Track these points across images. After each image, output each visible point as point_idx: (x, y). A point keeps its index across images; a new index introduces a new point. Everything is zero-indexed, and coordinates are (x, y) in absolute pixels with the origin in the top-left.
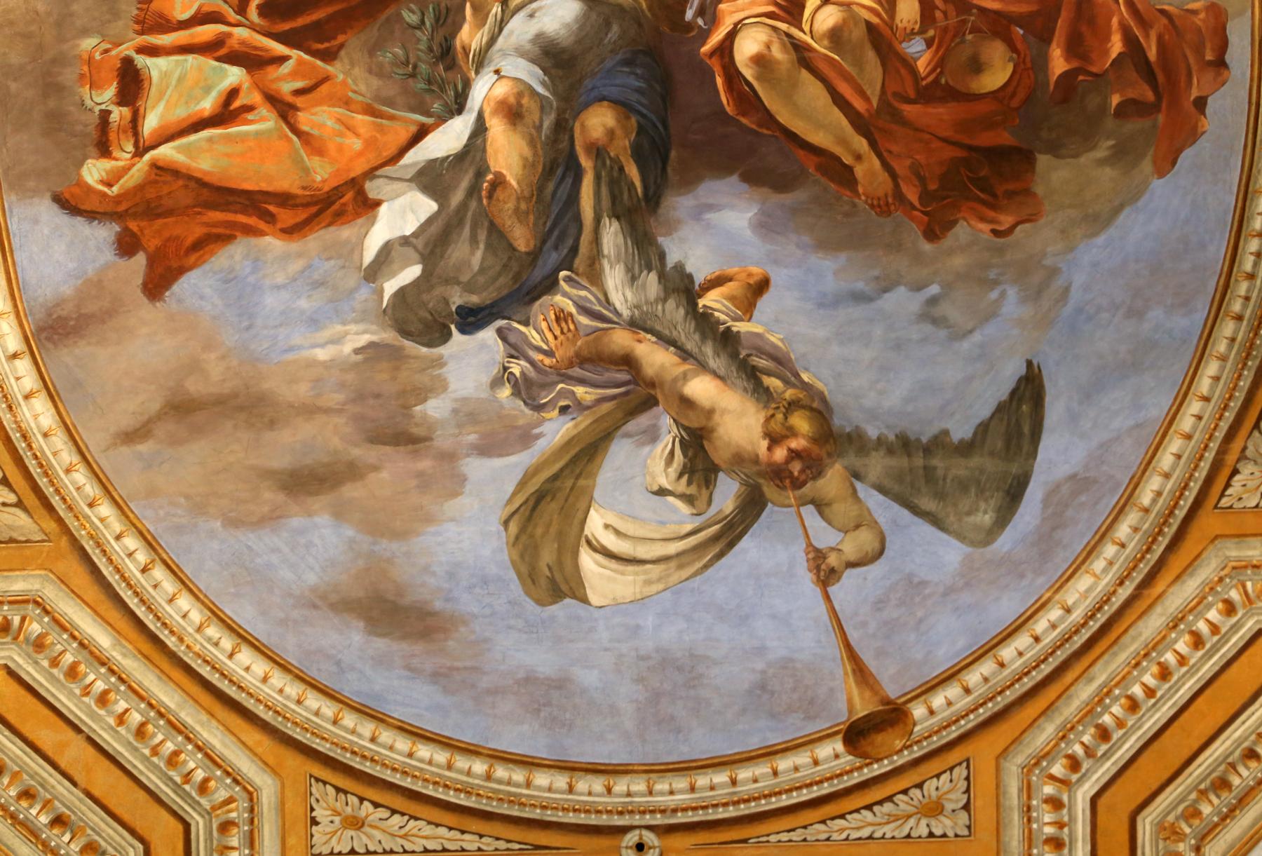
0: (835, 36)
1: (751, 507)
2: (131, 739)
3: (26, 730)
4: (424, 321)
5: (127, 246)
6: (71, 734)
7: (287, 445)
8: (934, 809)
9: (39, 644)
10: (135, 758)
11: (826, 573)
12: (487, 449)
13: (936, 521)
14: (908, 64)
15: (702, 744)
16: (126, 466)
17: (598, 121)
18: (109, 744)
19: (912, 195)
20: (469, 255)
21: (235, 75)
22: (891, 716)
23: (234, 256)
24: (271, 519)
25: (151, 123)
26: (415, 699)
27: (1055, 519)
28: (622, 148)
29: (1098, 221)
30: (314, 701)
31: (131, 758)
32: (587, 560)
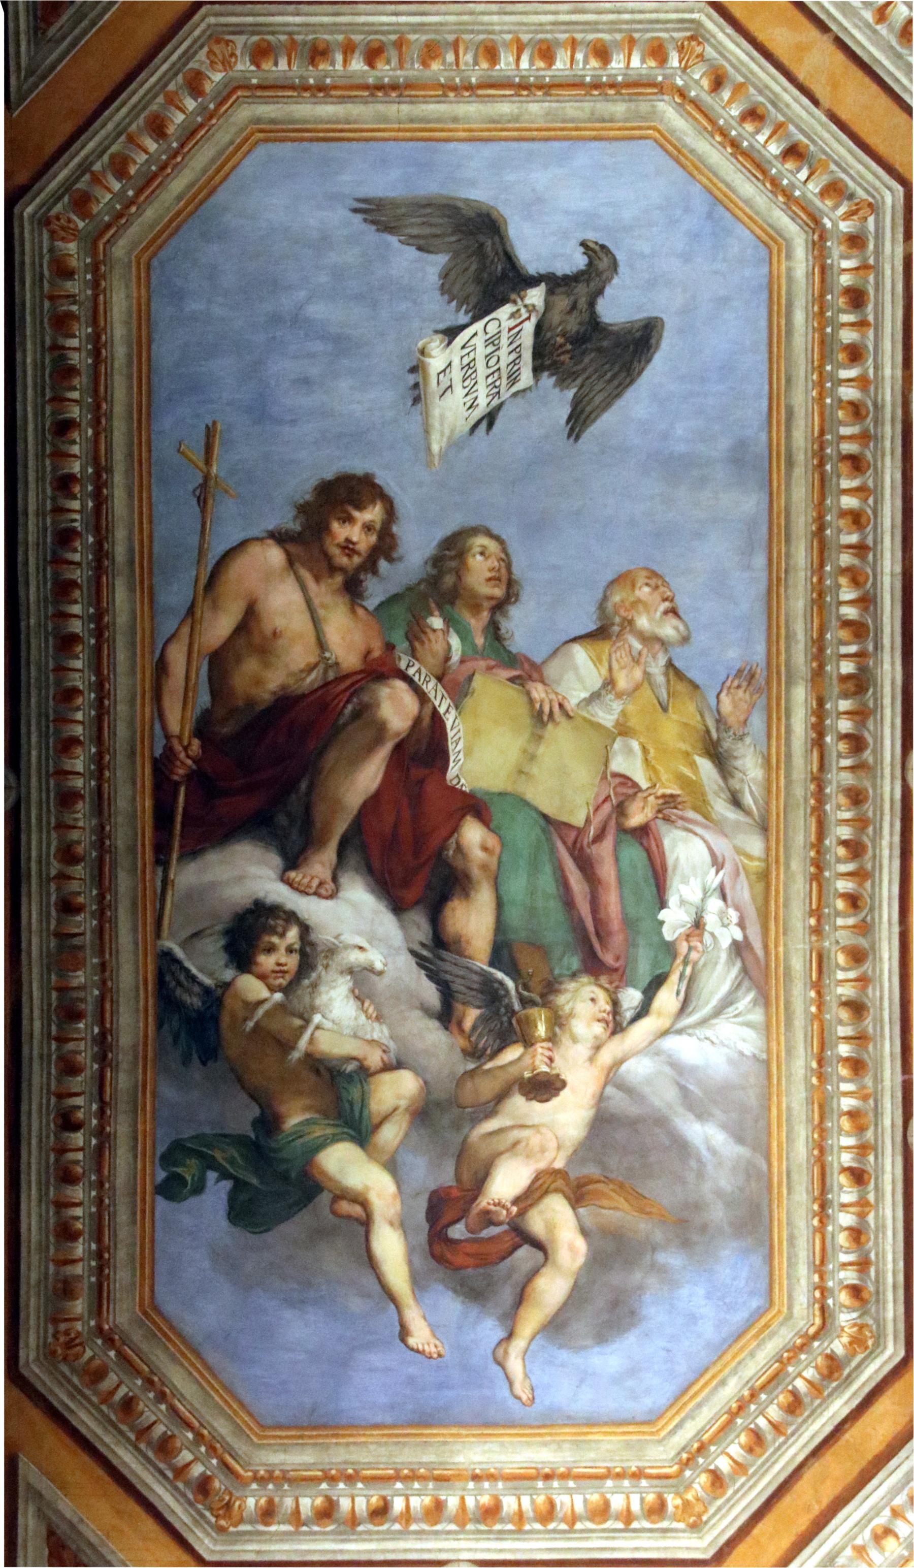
2: (894, 43)
3: (753, 27)
6: (814, 33)
10: (898, 68)
18: (863, 47)
31: (892, 68)
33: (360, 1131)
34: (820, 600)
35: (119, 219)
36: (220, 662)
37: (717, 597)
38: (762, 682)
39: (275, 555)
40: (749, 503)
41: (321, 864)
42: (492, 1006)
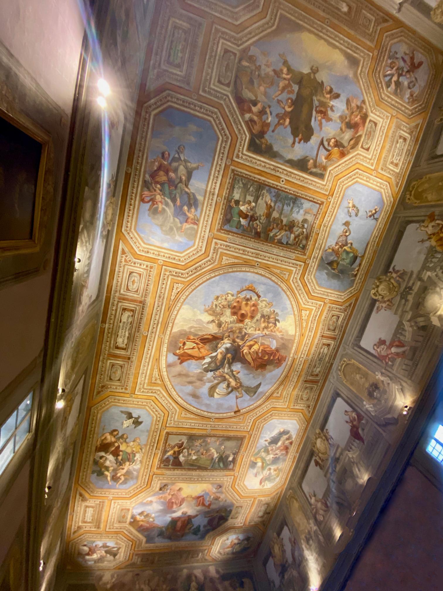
0: (253, 352)
1: (232, 391)
4: (207, 370)
5: (179, 359)
7: (189, 379)
8: (240, 419)
9: (159, 394)
11: (237, 398)
12: (209, 382)
13: (247, 394)
15: (221, 412)
16: (172, 380)
17: (229, 355)
20: (213, 365)
21: (195, 345)
22: (239, 411)
23: (189, 361)
24: (185, 385)
25: (185, 348)
27: (258, 395)
29: (271, 371)
30: (185, 403)
32: (215, 394)
33: (108, 471)
34: (151, 440)
35: (100, 409)
36: (103, 440)
37: (143, 439)
38: (146, 445)
39: (108, 434)
40: (147, 434)
41: (108, 454)
42: (120, 464)
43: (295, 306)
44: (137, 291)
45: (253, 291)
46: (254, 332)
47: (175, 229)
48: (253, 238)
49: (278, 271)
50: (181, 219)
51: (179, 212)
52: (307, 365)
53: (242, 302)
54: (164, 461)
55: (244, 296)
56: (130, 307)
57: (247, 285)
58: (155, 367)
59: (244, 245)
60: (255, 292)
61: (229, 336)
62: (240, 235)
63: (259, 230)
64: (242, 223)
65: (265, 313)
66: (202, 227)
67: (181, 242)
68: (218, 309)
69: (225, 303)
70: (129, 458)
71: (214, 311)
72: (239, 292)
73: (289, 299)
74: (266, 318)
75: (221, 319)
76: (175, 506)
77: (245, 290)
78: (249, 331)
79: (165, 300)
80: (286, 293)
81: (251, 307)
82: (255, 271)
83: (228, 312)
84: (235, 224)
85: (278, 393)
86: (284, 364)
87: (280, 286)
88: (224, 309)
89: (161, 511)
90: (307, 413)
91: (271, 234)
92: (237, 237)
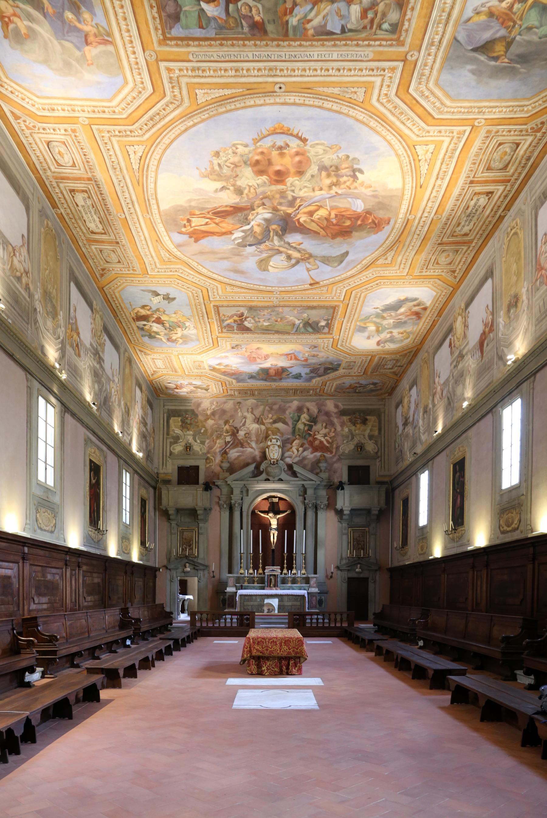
0: (319, 219)
1: (298, 262)
11: (308, 270)
14: (332, 222)
19: (330, 235)
21: (208, 220)
25: (193, 225)
26: (242, 279)
28: (278, 229)
32: (269, 267)
38: (193, 316)
43: (394, 141)
44: (74, 165)
45: (287, 132)
46: (312, 194)
47: (74, 63)
48: (249, 40)
49: (336, 91)
50: (75, 40)
51: (63, 29)
52: (439, 225)
53: (270, 154)
54: (225, 327)
55: (270, 144)
56: (77, 187)
57: (269, 126)
58: (159, 247)
59: (233, 58)
60: (291, 135)
61: (263, 204)
62: (215, 39)
63: (257, 18)
64: (210, 14)
65: (327, 163)
66: (124, 44)
67: (99, 83)
68: (226, 170)
69: (236, 159)
70: (179, 325)
71: (219, 175)
72: (256, 141)
73: (377, 132)
74: (332, 170)
75: (239, 183)
76: (259, 361)
77: (269, 135)
78: (302, 194)
79: (125, 171)
80: (367, 125)
81: (292, 157)
82: (278, 100)
83: (248, 172)
84: (193, 19)
85: (386, 259)
86: (388, 228)
87: (347, 115)
88: (238, 169)
89: (242, 363)
90: (450, 278)
91: (293, 21)
92: (210, 45)
